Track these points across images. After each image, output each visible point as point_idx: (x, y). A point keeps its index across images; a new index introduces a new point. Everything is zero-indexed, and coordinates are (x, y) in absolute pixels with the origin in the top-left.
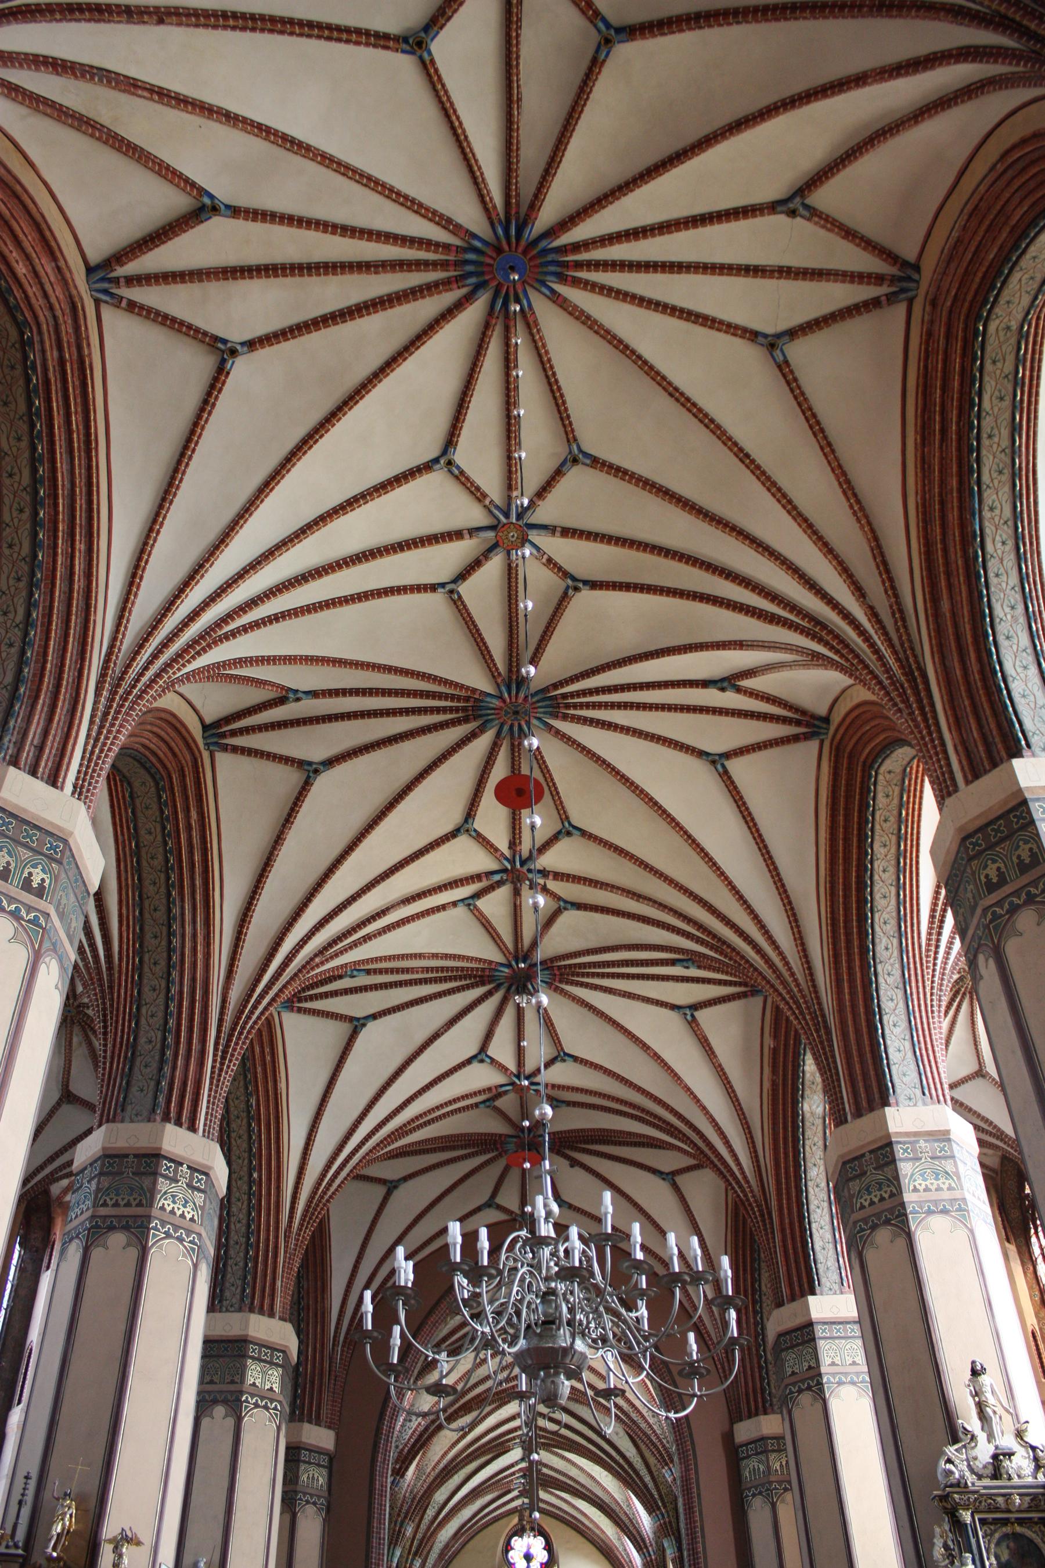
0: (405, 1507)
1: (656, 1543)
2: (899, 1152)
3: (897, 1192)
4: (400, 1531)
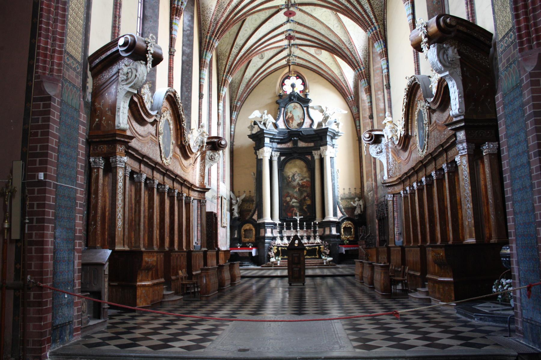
0: (212, 29)
1: (365, 63)
4: (209, 42)
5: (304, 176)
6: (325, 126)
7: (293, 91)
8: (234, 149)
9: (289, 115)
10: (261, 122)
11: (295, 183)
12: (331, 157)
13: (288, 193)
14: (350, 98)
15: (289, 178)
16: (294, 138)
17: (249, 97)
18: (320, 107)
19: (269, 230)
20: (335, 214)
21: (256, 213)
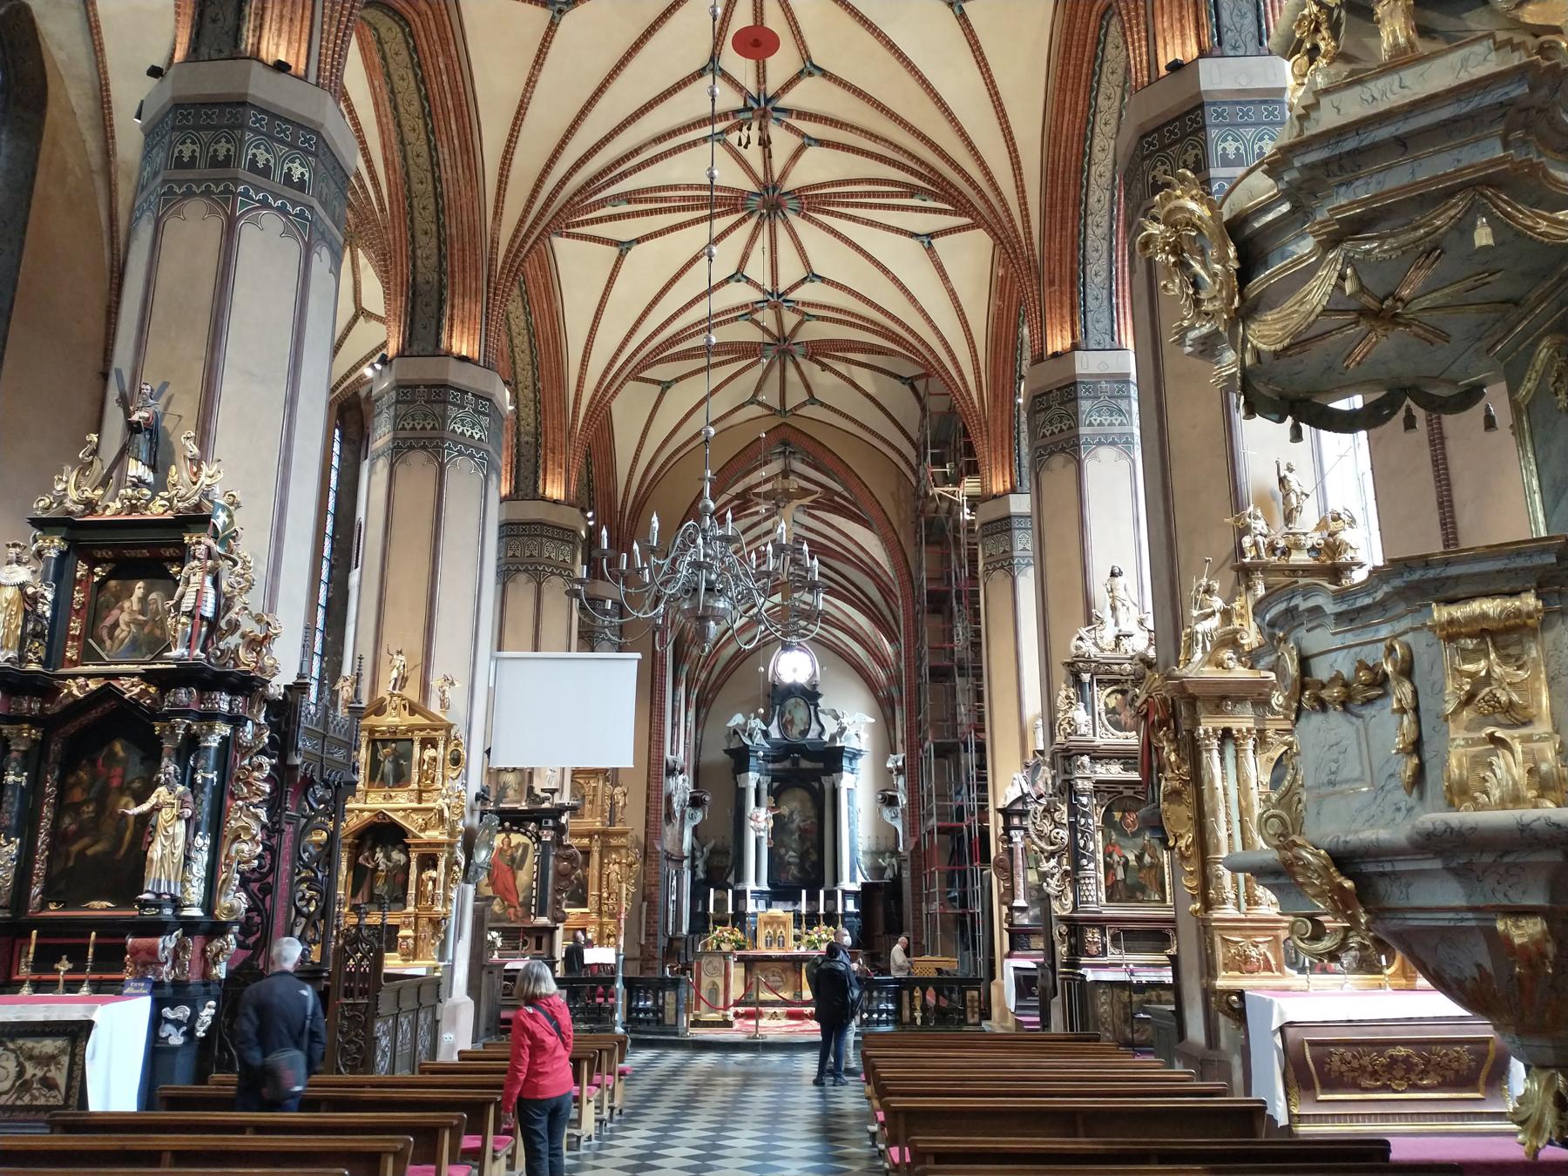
2: (1082, 392)
3: (1074, 427)
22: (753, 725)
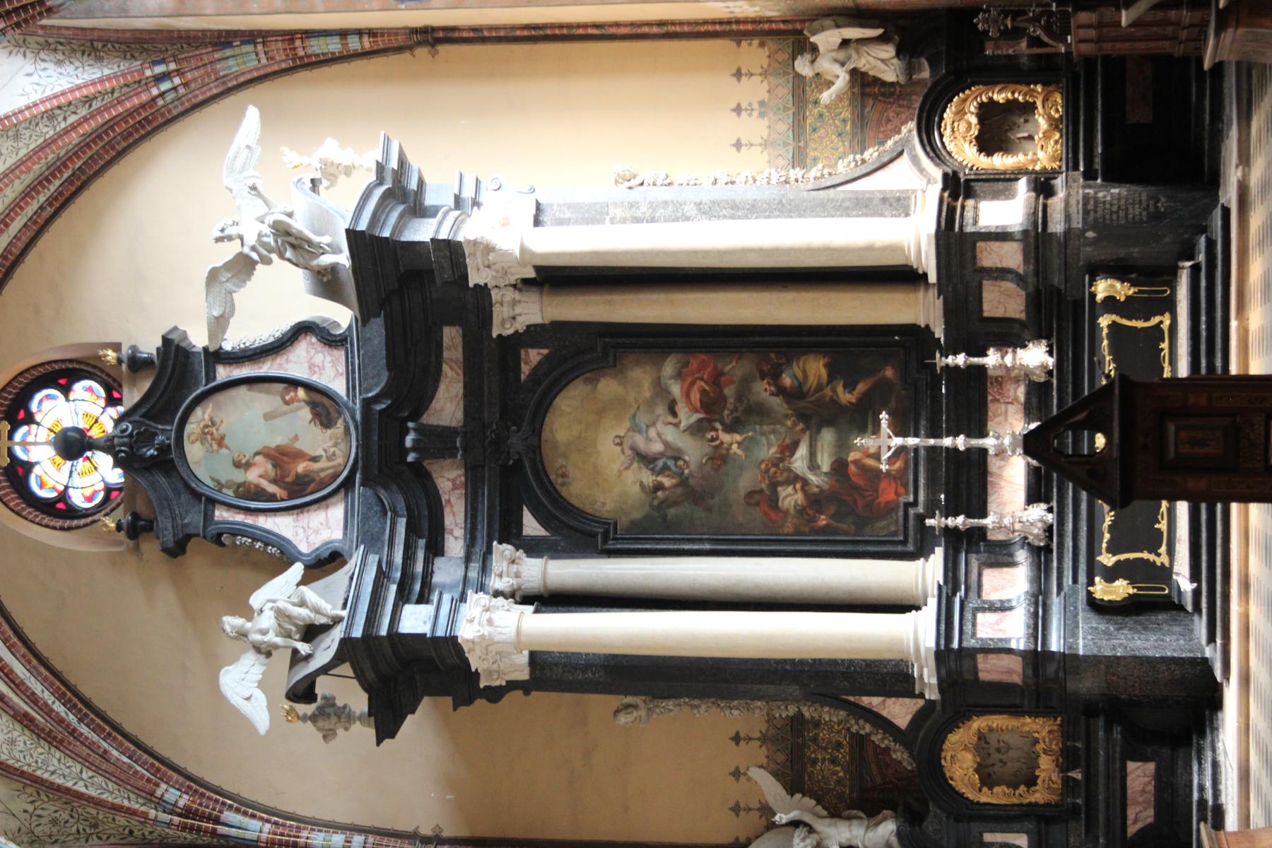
5: (647, 393)
6: (335, 250)
7: (108, 446)
8: (464, 832)
9: (253, 476)
10: (295, 652)
11: (694, 452)
12: (537, 222)
13: (750, 495)
14: (165, 86)
15: (659, 487)
16: (406, 452)
17: (129, 728)
18: (213, 276)
19: (988, 627)
20: (898, 204)
21: (873, 702)
22: (267, 620)
